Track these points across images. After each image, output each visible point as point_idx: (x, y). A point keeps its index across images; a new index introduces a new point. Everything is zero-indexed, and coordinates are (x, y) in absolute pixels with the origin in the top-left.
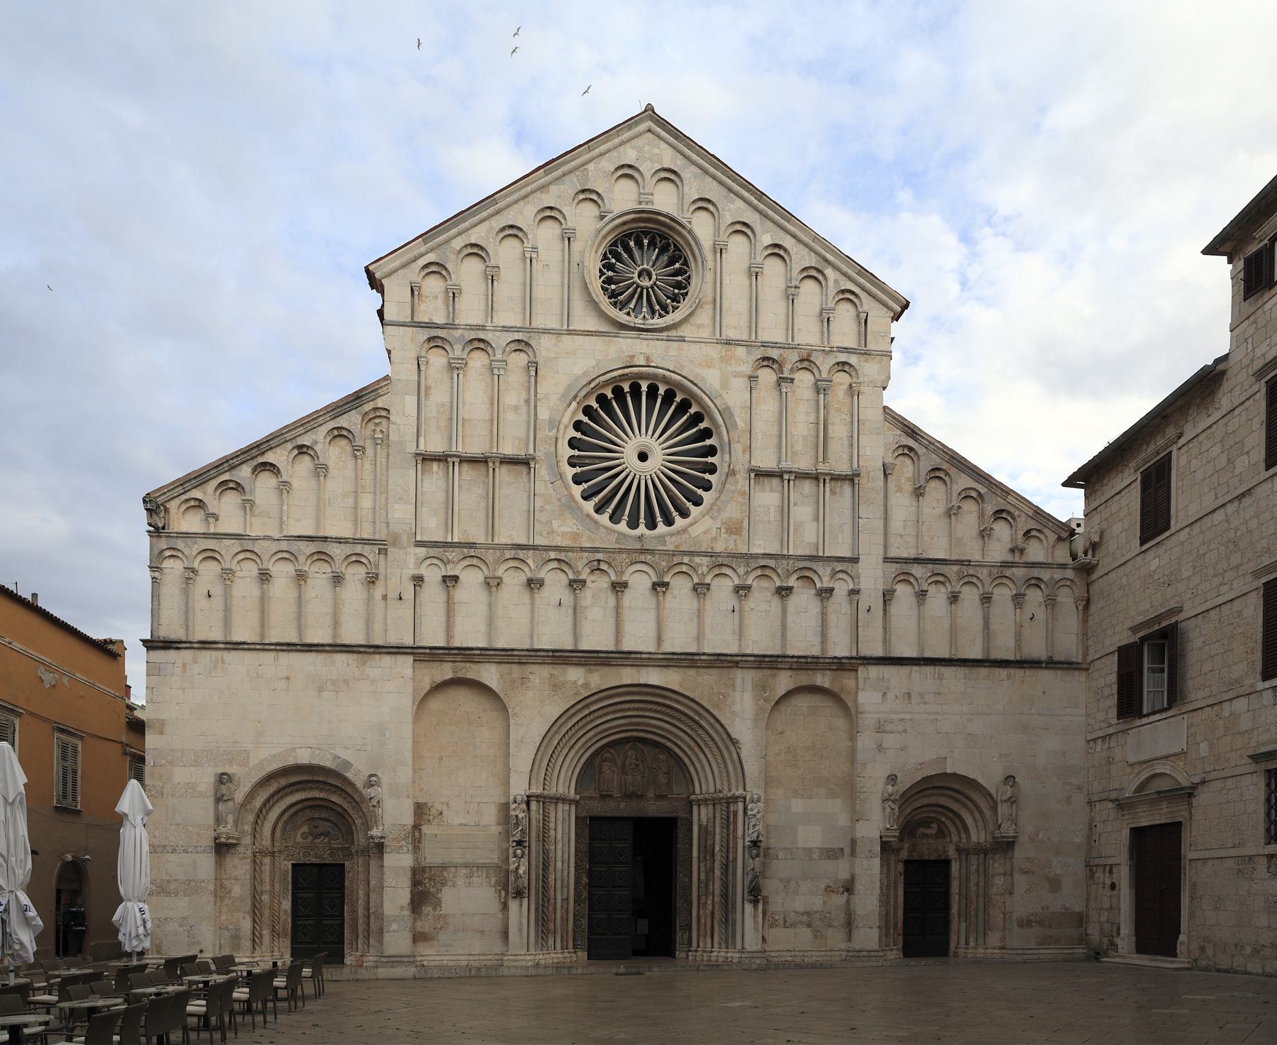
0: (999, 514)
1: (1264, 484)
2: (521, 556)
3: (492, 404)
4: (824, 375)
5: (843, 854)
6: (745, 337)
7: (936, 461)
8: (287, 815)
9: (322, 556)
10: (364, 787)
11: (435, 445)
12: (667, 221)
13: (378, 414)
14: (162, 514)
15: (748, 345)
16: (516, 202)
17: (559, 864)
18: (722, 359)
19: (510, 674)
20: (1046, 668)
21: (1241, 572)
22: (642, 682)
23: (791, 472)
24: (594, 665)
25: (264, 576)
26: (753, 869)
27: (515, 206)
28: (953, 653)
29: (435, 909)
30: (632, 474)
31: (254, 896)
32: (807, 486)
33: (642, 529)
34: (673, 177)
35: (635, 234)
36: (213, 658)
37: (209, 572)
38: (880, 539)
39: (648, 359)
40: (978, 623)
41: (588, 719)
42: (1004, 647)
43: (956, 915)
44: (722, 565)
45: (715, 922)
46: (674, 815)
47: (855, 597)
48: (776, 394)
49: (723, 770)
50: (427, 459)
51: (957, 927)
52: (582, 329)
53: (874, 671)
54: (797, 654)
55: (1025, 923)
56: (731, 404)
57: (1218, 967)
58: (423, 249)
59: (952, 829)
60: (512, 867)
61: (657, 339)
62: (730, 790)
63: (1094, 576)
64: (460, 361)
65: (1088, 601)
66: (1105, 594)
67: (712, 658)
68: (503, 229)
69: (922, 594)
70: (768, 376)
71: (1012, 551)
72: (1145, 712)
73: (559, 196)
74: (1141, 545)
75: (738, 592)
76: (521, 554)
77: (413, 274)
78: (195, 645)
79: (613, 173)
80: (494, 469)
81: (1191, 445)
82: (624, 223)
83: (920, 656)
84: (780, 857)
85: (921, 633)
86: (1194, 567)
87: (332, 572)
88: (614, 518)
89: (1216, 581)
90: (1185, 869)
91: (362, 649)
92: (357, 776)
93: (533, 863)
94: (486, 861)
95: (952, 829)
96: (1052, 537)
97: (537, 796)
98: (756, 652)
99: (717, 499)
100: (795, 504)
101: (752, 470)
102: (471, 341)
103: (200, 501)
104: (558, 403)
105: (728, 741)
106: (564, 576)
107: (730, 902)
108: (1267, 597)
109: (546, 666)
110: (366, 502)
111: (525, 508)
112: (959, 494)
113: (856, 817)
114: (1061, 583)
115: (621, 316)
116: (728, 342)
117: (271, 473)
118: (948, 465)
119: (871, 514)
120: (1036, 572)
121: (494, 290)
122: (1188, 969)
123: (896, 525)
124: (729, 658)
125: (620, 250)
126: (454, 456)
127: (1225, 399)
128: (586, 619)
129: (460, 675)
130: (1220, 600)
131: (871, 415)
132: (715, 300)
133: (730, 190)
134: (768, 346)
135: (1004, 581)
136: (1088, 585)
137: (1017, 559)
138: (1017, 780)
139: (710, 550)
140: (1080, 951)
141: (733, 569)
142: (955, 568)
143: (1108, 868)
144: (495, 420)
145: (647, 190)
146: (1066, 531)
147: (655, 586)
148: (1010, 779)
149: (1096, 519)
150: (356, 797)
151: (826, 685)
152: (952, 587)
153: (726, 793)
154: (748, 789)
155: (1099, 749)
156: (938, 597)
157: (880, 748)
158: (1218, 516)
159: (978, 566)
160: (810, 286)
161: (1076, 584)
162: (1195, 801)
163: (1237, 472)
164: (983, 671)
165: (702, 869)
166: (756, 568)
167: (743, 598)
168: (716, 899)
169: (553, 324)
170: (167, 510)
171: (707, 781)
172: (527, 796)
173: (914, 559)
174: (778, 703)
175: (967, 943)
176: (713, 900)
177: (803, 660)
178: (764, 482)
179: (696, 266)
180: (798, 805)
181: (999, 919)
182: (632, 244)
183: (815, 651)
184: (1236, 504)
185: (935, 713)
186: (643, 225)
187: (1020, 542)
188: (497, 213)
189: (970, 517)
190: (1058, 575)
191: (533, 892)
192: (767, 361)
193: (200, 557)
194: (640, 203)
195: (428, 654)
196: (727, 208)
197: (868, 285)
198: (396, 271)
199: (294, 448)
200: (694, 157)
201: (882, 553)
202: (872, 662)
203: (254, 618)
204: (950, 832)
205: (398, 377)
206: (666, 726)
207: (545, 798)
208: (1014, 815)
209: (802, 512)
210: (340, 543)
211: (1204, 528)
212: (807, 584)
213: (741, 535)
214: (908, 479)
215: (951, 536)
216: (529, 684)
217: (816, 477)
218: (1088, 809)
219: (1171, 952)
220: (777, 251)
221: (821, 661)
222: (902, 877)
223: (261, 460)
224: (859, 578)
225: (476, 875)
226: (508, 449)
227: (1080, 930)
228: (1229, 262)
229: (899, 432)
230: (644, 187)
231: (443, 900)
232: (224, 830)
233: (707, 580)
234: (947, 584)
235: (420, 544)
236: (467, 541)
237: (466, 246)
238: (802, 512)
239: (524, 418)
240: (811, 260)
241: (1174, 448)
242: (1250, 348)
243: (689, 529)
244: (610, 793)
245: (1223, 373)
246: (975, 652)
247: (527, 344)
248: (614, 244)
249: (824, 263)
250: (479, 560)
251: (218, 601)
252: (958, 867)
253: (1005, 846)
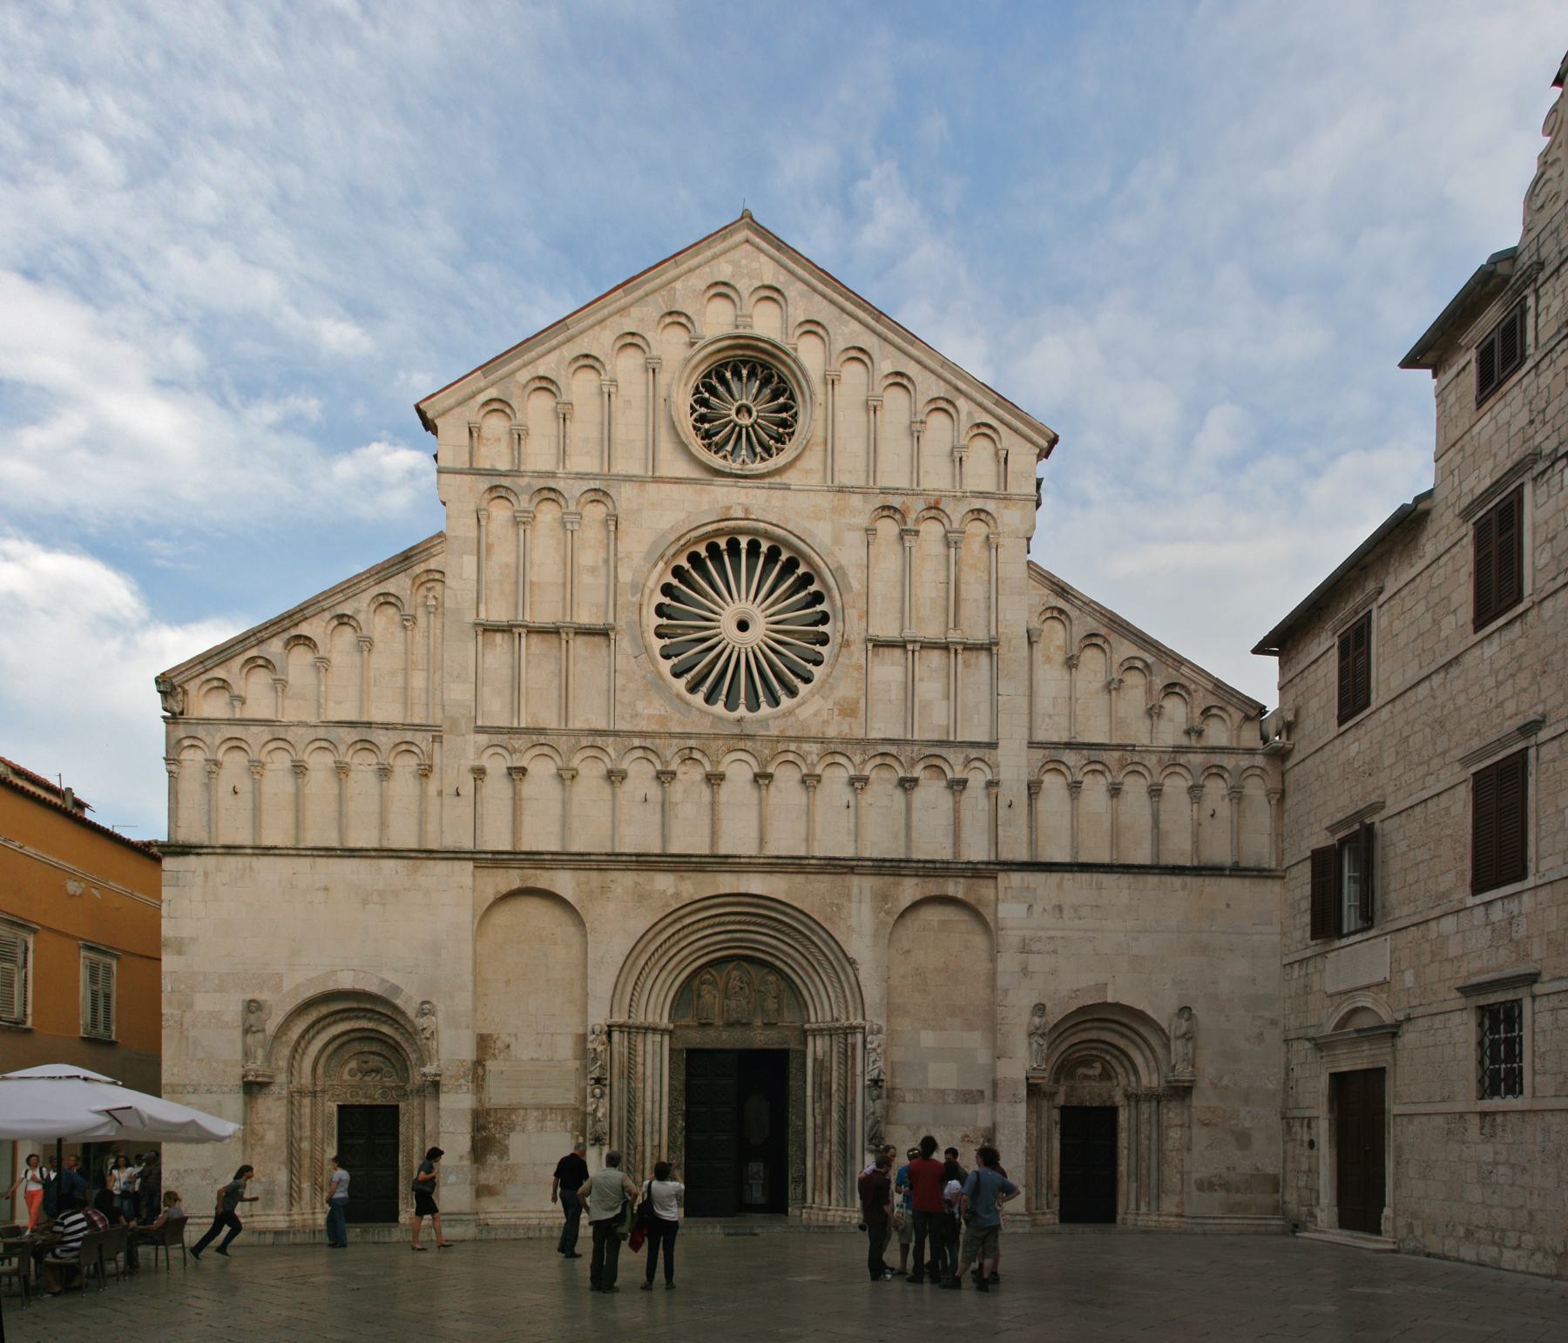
0: (1170, 689)
1: (1473, 650)
2: (599, 744)
3: (565, 565)
4: (956, 525)
5: (984, 1097)
6: (862, 483)
7: (1092, 625)
8: (331, 1048)
9: (367, 745)
10: (417, 1016)
11: (498, 613)
12: (769, 347)
13: (431, 577)
14: (180, 697)
15: (864, 492)
16: (591, 327)
17: (648, 1105)
18: (834, 510)
19: (588, 882)
20: (1230, 876)
21: (1448, 760)
22: (742, 890)
23: (915, 642)
25: (299, 769)
26: (873, 1113)
27: (591, 332)
28: (1115, 857)
29: (501, 1158)
30: (730, 646)
31: (292, 1143)
32: (936, 657)
33: (742, 711)
34: (775, 295)
35: (731, 364)
36: (240, 866)
37: (234, 764)
38: (1025, 720)
39: (747, 510)
40: (1146, 819)
41: (681, 934)
42: (1179, 850)
43: (1125, 1173)
44: (835, 752)
45: (833, 1174)
46: (786, 1046)
47: (994, 790)
48: (898, 548)
49: (840, 995)
50: (489, 629)
51: (1126, 1188)
52: (669, 475)
53: (1016, 878)
54: (923, 857)
55: (1206, 1186)
56: (844, 562)
57: (1427, 1250)
58: (482, 384)
59: (1120, 1070)
60: (590, 1109)
61: (758, 488)
62: (848, 1019)
63: (1289, 764)
64: (526, 515)
65: (1283, 795)
66: (1302, 786)
67: (822, 862)
68: (577, 359)
69: (1075, 787)
70: (888, 528)
71: (1188, 733)
72: (1345, 931)
73: (642, 320)
74: (1339, 725)
75: (853, 785)
76: (599, 741)
77: (472, 412)
78: (219, 851)
79: (705, 291)
80: (567, 642)
81: (1393, 603)
82: (719, 351)
83: (1074, 861)
84: (907, 1099)
85: (1075, 833)
86: (1397, 753)
87: (378, 764)
88: (710, 699)
89: (1422, 770)
90: (1389, 1125)
91: (413, 854)
92: (408, 1002)
93: (615, 1104)
94: (560, 1102)
95: (1120, 1070)
96: (1237, 716)
97: (620, 1026)
98: (875, 855)
99: (829, 675)
100: (921, 680)
101: (868, 640)
102: (540, 490)
103: (224, 681)
104: (642, 563)
105: (844, 961)
106: (650, 767)
107: (849, 1153)
108: (1476, 790)
109: (629, 872)
110: (418, 681)
111: (605, 687)
112: (1121, 665)
113: (998, 1054)
114: (1250, 772)
115: (716, 461)
116: (841, 490)
117: (306, 648)
118: (1106, 629)
119: (1013, 691)
120: (1217, 759)
121: (567, 430)
122: (1393, 1251)
123: (1044, 703)
124: (842, 863)
125: (714, 382)
126: (520, 626)
127: (1429, 546)
128: (677, 817)
129: (530, 884)
130: (1426, 794)
131: (1013, 570)
132: (826, 440)
133: (843, 310)
134: (889, 493)
135: (1178, 769)
136: (1283, 774)
137: (1194, 743)
138: (1194, 1011)
139: (820, 735)
140: (1276, 1222)
141: (848, 757)
142: (1116, 754)
143: (1306, 1121)
144: (569, 583)
145: (744, 312)
146: (1254, 709)
147: (757, 777)
148: (1185, 1011)
149: (1292, 693)
150: (408, 1027)
151: (960, 895)
152: (1113, 777)
153: (844, 1022)
154: (867, 1018)
155: (1295, 976)
156: (1095, 791)
157: (1025, 971)
158: (1424, 689)
159: (1145, 751)
160: (938, 420)
161: (1267, 773)
162: (1399, 1043)
163: (1443, 635)
164: (1152, 880)
165: (817, 1111)
166: (875, 756)
167: (859, 791)
168: (834, 1148)
169: (636, 469)
170: (185, 692)
171: (823, 1009)
172: (609, 1026)
173: (1066, 744)
174: (902, 915)
175: (1138, 1208)
176: (830, 1149)
177: (930, 865)
178: (883, 654)
179: (804, 401)
180: (928, 1038)
181: (1175, 1180)
182: (728, 375)
183: (946, 854)
184: (1442, 675)
185: (1093, 930)
186: (740, 352)
187: (1197, 723)
188: (569, 340)
189: (1135, 691)
190: (1245, 761)
191: (615, 1138)
192: (888, 510)
193: (224, 747)
194: (737, 327)
195: (491, 859)
196: (840, 331)
197: (1008, 417)
198: (451, 409)
199: (333, 618)
200: (800, 271)
201: (1026, 736)
203: (288, 818)
204: (1115, 1071)
205: (454, 534)
206: (774, 942)
207: (630, 1027)
208: (1190, 1055)
209: (930, 689)
210: (387, 729)
211: (1408, 706)
212: (936, 775)
213: (856, 717)
214: (1059, 648)
215: (1111, 716)
216: (609, 895)
217: (945, 647)
218: (1284, 1048)
219: (1374, 1228)
220: (899, 380)
221: (953, 866)
222: (1058, 1126)
223: (294, 632)
224: (998, 766)
225: (549, 1118)
226: (585, 618)
227: (1276, 1196)
228: (1435, 376)
229: (1047, 592)
230: (741, 308)
231: (511, 1147)
232: (253, 1066)
233: (818, 771)
234: (1107, 774)
235: (480, 730)
236: (537, 726)
237: (533, 379)
238: (930, 689)
239: (602, 581)
240: (938, 389)
241: (1374, 606)
242: (1457, 482)
243: (797, 711)
244: (710, 1021)
245: (1427, 513)
246: (1143, 856)
247: (605, 493)
248: (708, 375)
249: (957, 394)
250: (550, 749)
251: (246, 799)
252: (1127, 1115)
253: (1181, 1092)
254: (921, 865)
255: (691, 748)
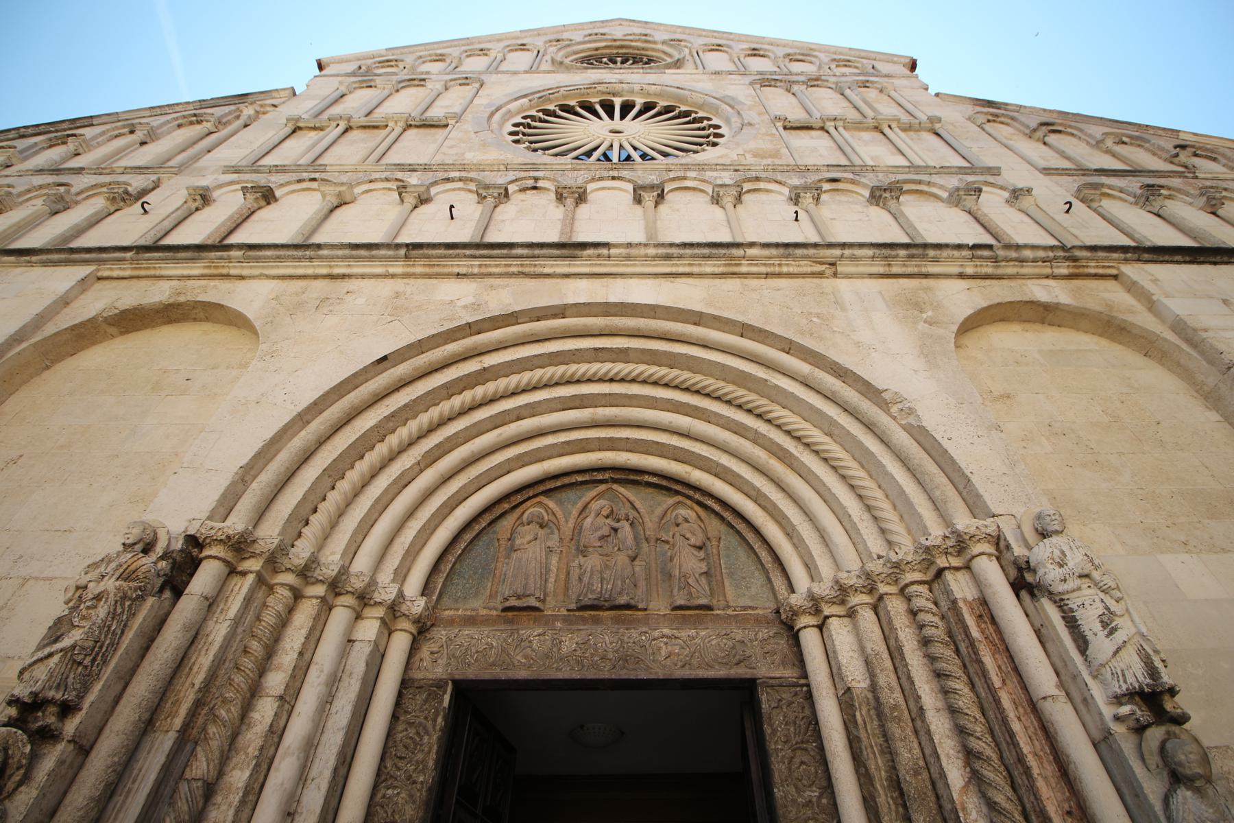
24: (500, 275)
67: (774, 252)
124: (812, 252)
202: (1146, 256)
254: (966, 253)
255: (536, 179)
